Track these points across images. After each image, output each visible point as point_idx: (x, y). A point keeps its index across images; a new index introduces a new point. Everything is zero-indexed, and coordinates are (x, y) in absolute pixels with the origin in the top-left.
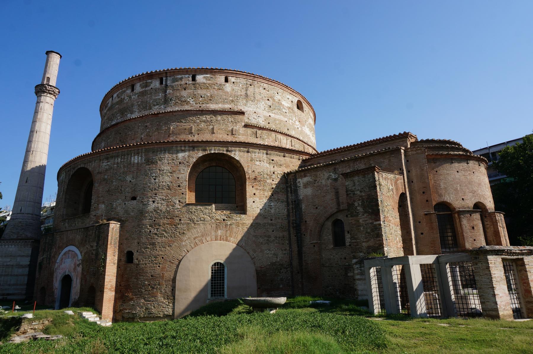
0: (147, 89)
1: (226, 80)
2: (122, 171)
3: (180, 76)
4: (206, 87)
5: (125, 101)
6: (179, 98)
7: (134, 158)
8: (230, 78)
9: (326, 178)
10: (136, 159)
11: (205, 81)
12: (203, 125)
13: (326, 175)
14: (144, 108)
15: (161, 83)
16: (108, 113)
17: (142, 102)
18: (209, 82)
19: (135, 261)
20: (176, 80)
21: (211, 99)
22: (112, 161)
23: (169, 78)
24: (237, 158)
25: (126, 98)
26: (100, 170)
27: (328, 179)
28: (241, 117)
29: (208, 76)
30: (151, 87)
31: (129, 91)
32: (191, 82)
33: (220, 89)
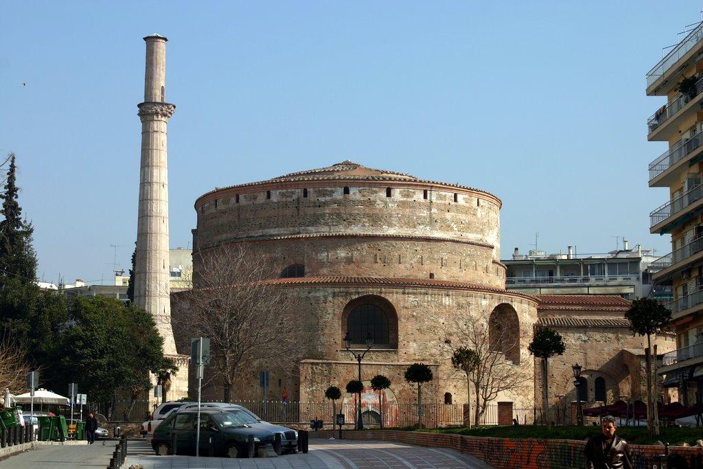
0: (408, 200)
1: (478, 205)
2: (433, 311)
3: (443, 193)
4: (467, 211)
5: (378, 206)
6: (444, 220)
7: (445, 299)
8: (480, 200)
9: (576, 338)
10: (447, 301)
11: (464, 204)
12: (468, 260)
13: (577, 335)
14: (406, 224)
15: (425, 197)
16: (335, 206)
17: (402, 215)
18: (467, 205)
19: (453, 402)
20: (440, 197)
21: (468, 227)
22: (419, 298)
23: (433, 193)
24: (516, 309)
25: (378, 202)
26: (406, 305)
27: (579, 338)
28: (489, 251)
29: (467, 196)
30: (413, 199)
31: (383, 194)
32: (454, 203)
33: (474, 215)
